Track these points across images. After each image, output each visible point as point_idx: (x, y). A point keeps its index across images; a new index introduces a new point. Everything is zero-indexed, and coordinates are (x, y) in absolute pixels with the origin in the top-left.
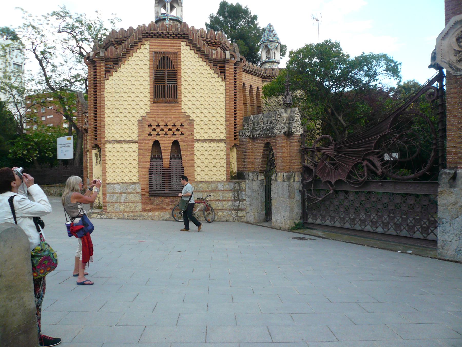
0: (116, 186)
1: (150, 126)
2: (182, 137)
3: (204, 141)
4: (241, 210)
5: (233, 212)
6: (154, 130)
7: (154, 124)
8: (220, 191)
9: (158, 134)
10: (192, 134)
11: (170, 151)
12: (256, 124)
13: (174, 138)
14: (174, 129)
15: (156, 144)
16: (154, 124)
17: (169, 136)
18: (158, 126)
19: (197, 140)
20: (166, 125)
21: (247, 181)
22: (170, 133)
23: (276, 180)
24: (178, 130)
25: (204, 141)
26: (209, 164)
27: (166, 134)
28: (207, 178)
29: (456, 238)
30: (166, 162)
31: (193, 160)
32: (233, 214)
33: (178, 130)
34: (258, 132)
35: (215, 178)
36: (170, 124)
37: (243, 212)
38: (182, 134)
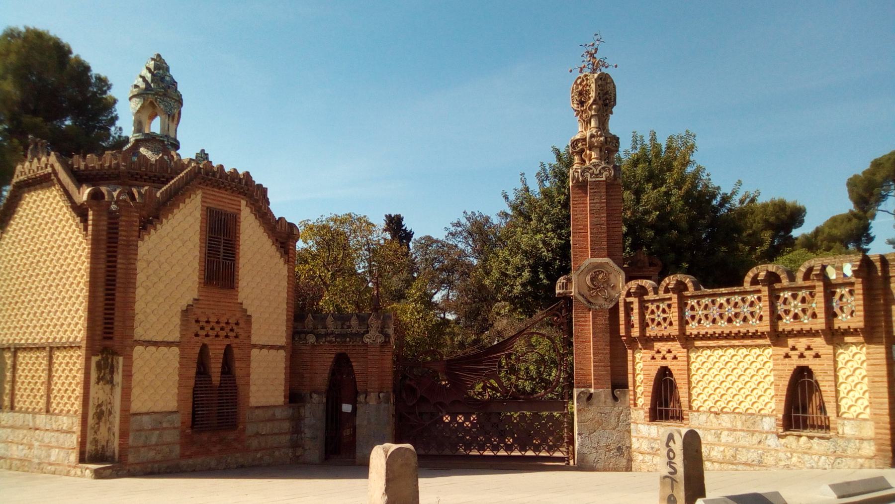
0: (146, 419)
1: (197, 321)
2: (237, 341)
3: (262, 347)
4: (299, 446)
5: (290, 450)
6: (202, 328)
7: (203, 319)
8: (277, 420)
9: (207, 335)
10: (249, 337)
11: (221, 361)
12: (320, 327)
13: (227, 342)
14: (228, 329)
15: (204, 349)
16: (203, 319)
17: (221, 338)
18: (208, 322)
19: (255, 346)
20: (218, 322)
21: (309, 405)
22: (223, 333)
23: (367, 403)
24: (232, 330)
25: (262, 347)
26: (265, 380)
27: (217, 336)
28: (263, 402)
29: (594, 451)
30: (216, 378)
31: (248, 375)
32: (290, 452)
33: (232, 330)
34: (328, 339)
35: (272, 401)
36: (223, 320)
37: (301, 449)
38: (236, 337)
